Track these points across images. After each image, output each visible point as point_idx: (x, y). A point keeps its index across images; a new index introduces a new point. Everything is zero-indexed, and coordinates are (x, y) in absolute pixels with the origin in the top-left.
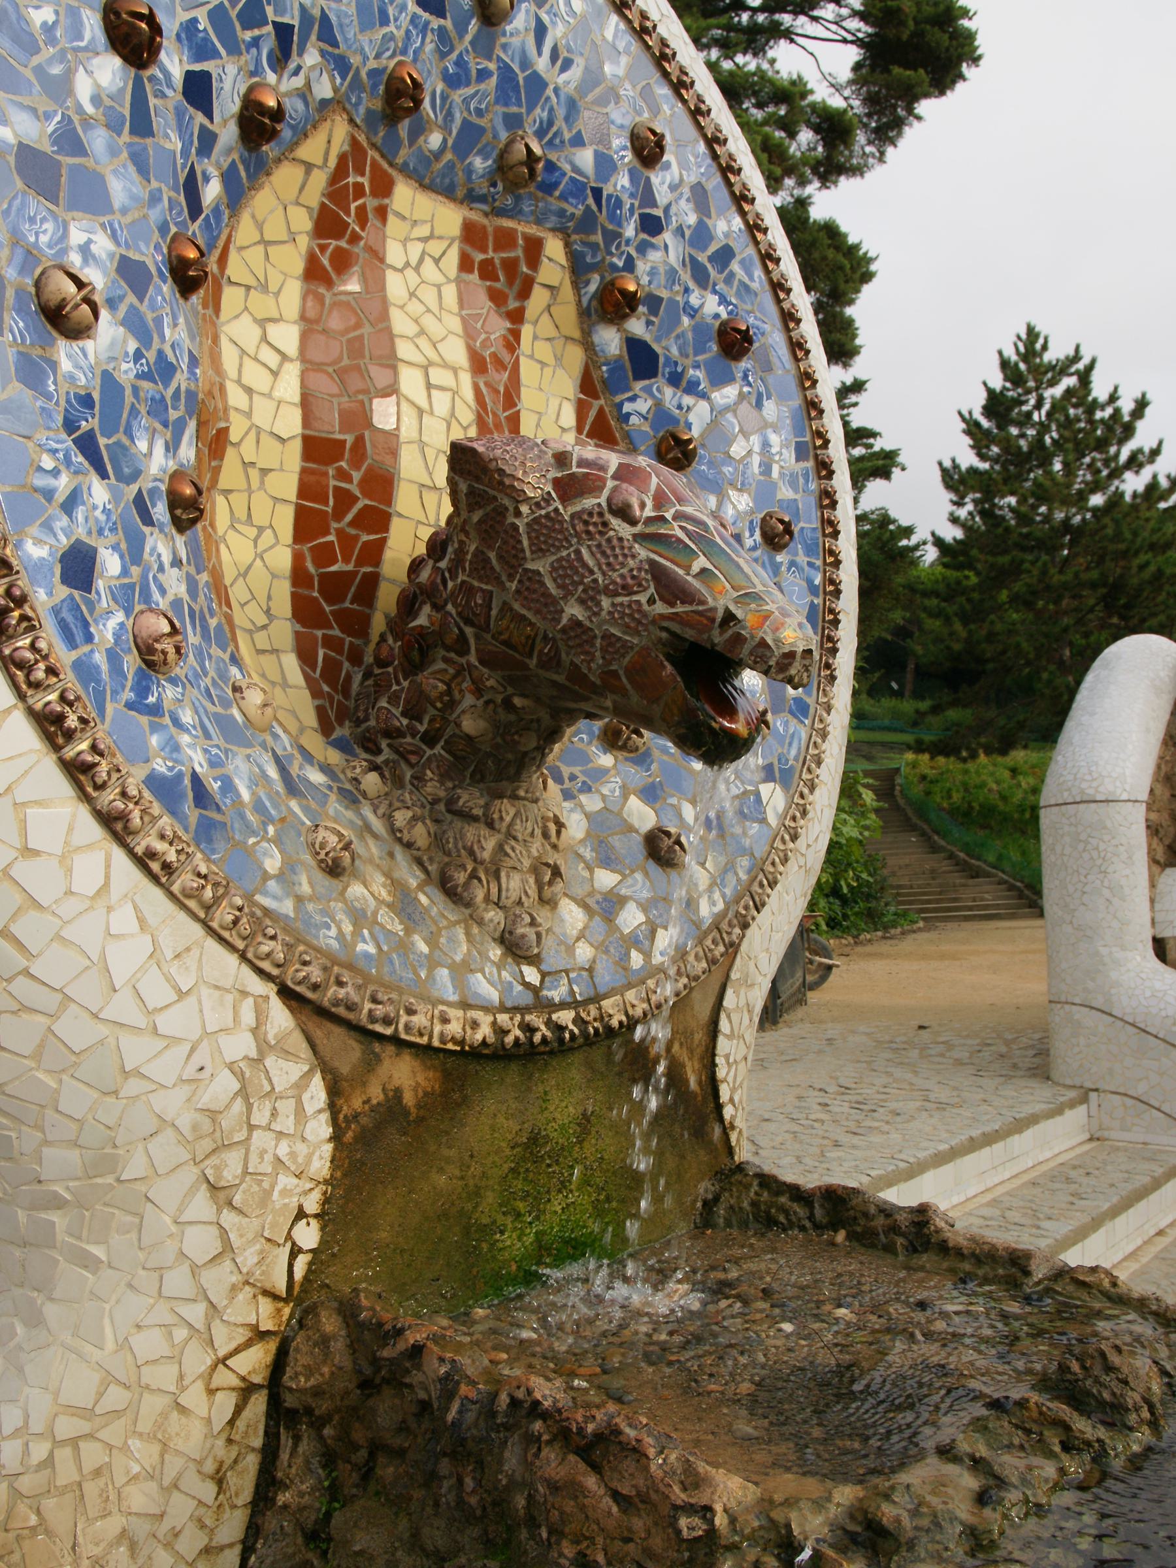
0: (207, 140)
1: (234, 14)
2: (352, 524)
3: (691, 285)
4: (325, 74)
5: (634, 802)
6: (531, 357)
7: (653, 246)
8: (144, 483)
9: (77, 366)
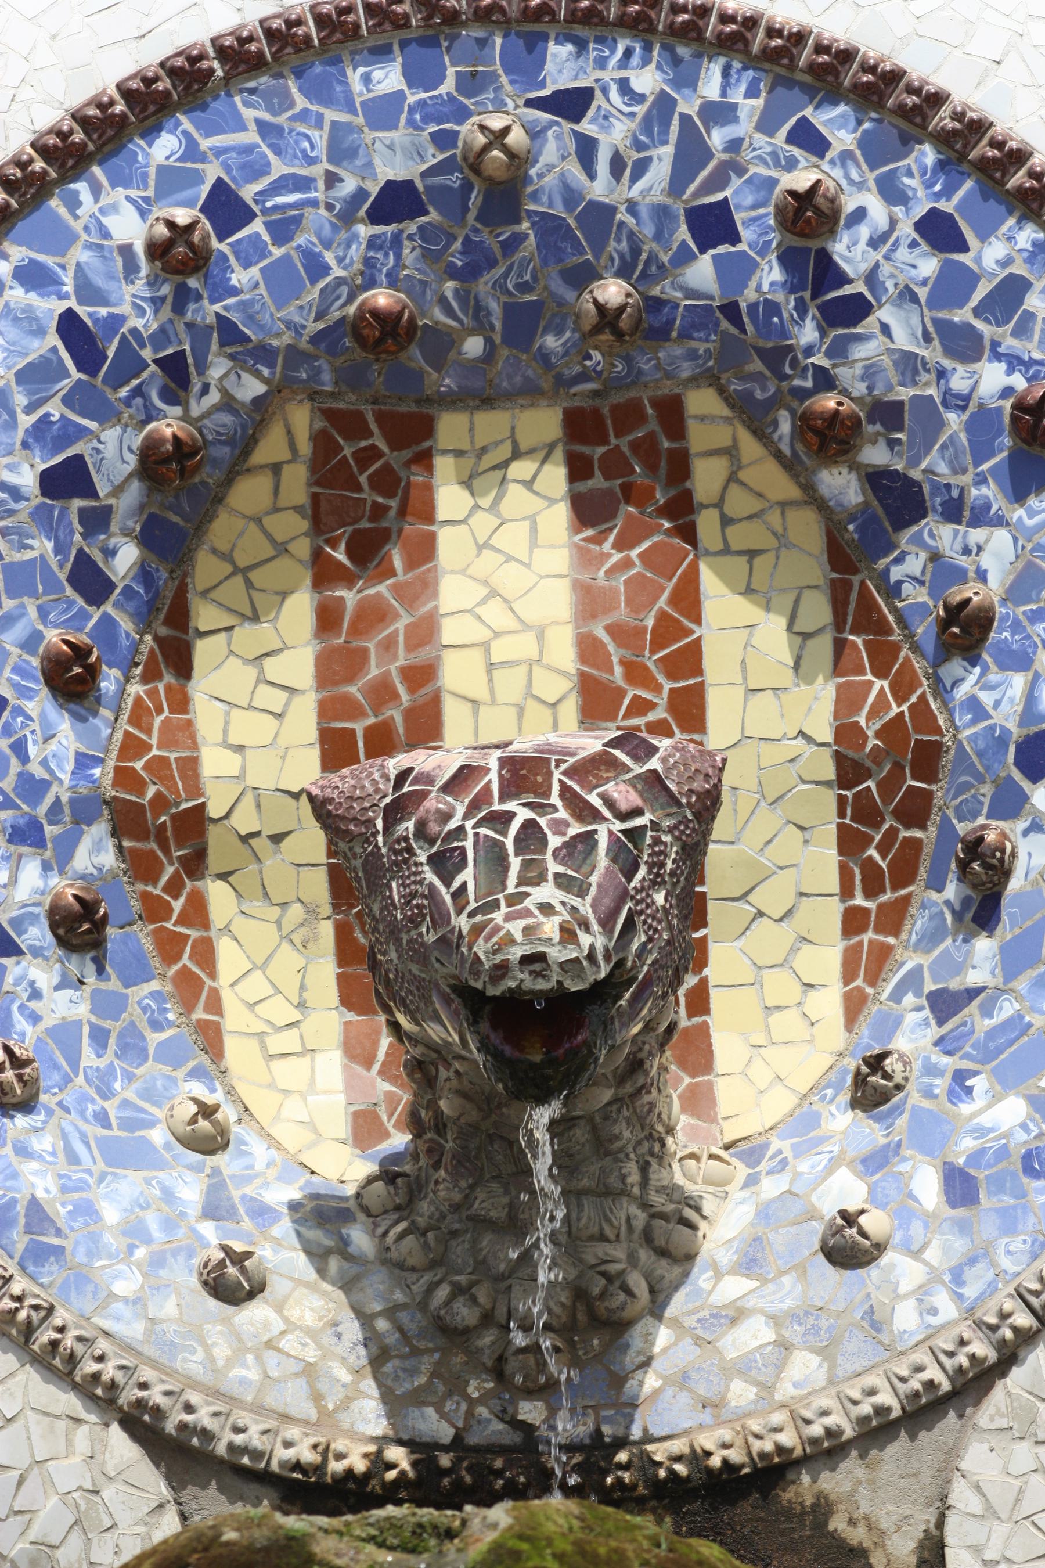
3: (947, 363)
4: (246, 376)
6: (726, 550)
7: (859, 338)
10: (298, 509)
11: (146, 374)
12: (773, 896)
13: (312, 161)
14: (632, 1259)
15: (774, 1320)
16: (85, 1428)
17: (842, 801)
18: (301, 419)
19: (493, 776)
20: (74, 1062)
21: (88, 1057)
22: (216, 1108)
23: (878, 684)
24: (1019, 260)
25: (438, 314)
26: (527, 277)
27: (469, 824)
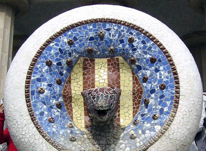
0: (62, 68)
1: (62, 55)
3: (144, 55)
4: (77, 55)
6: (123, 73)
8: (52, 105)
9: (43, 96)
10: (81, 68)
11: (67, 54)
12: (126, 106)
13: (84, 35)
14: (112, 139)
15: (125, 144)
17: (133, 97)
18: (82, 59)
19: (99, 90)
20: (58, 118)
21: (60, 118)
22: (72, 124)
23: (137, 85)
24: (151, 45)
25: (95, 50)
26: (104, 46)
27: (96, 94)
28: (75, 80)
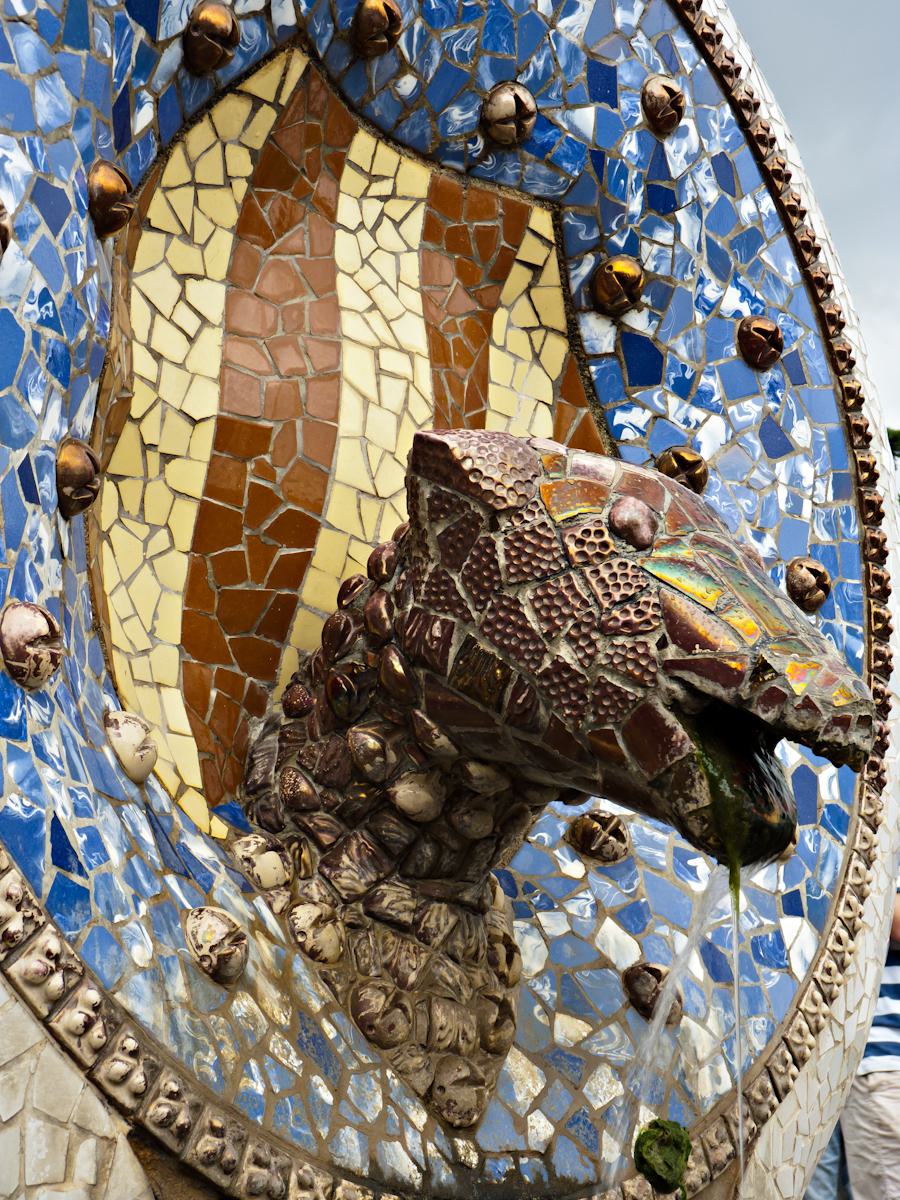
2: (268, 532)
3: (708, 274)
5: (610, 928)
6: (503, 348)
10: (252, 152)
16: (91, 1142)
18: (299, 64)
26: (468, 49)
28: (175, 241)
